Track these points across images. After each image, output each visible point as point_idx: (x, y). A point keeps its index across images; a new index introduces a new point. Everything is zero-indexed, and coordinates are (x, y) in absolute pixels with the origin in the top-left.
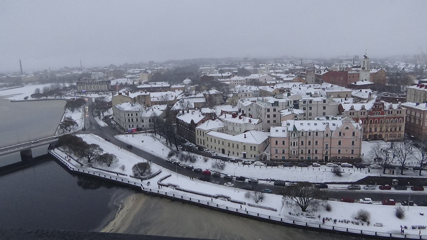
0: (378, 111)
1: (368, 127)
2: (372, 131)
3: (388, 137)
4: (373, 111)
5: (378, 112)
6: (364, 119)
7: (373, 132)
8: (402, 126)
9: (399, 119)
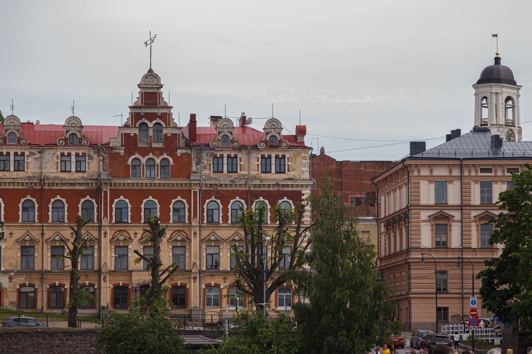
0: (159, 152)
2: (130, 269)
5: (158, 161)
6: (83, 194)
7: (131, 272)
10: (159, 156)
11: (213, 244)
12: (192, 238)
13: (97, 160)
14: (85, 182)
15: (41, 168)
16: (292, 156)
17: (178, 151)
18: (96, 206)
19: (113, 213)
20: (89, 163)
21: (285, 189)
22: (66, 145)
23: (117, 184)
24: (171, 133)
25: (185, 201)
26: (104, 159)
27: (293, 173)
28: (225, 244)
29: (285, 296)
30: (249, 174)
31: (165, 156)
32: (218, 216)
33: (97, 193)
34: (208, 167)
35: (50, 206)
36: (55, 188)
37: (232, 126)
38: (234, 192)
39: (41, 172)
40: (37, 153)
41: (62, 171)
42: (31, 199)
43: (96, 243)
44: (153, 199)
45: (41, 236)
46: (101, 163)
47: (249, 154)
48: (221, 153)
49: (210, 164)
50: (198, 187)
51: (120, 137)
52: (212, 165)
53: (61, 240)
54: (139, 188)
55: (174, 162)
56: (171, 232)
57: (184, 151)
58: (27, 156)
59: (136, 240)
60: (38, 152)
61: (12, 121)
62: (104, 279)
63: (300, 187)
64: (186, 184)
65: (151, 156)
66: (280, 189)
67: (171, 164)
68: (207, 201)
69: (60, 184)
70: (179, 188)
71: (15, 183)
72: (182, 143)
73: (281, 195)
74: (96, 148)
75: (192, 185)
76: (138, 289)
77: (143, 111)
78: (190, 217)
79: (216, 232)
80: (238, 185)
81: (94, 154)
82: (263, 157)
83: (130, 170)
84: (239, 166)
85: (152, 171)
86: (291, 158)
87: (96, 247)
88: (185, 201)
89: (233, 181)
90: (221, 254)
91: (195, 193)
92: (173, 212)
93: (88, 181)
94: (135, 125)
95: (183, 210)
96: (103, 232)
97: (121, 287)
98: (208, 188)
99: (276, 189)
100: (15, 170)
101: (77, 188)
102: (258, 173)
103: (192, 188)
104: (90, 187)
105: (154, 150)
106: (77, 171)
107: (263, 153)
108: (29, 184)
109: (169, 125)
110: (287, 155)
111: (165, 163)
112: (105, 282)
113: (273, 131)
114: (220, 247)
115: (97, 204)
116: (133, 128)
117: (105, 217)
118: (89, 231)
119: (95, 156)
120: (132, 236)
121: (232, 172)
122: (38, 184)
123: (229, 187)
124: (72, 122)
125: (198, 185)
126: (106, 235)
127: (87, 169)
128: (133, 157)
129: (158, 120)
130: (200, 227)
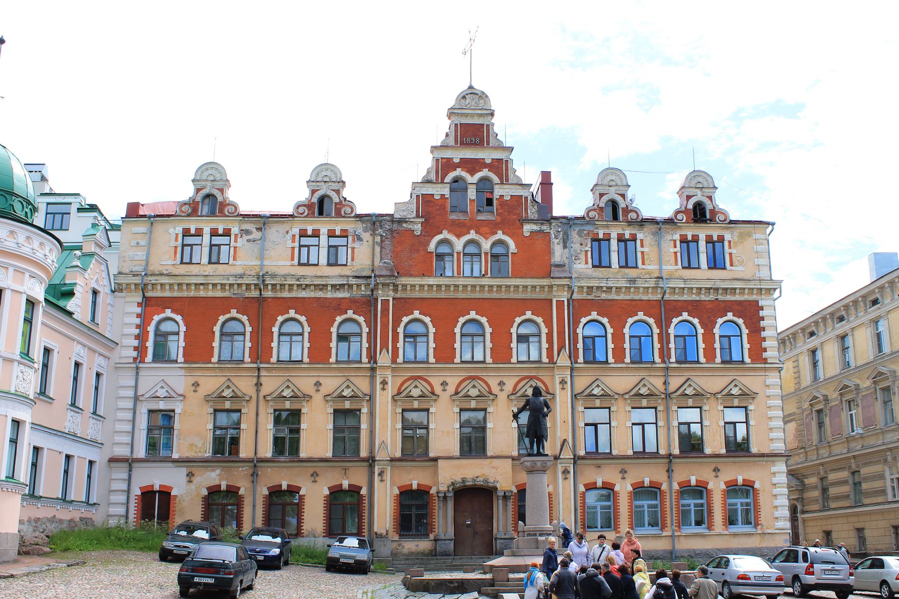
1: (384, 400)
2: (432, 454)
3: (624, 527)
4: (430, 229)
5: (486, 245)
6: (339, 306)
7: (435, 460)
8: (747, 395)
9: (709, 326)
10: (487, 235)
11: (598, 403)
12: (558, 391)
13: (371, 242)
14: (345, 283)
15: (262, 258)
16: (736, 238)
17: (525, 227)
18: (366, 330)
19: (400, 345)
20: (353, 249)
21: (729, 298)
22: (311, 214)
23: (409, 288)
24: (510, 194)
25: (539, 320)
26: (382, 241)
27: (740, 268)
28: (621, 402)
29: (739, 506)
30: (660, 270)
31: (500, 235)
32: (606, 350)
33: (367, 306)
34: (582, 256)
35: (275, 330)
36: (286, 294)
37: (625, 184)
38: (633, 303)
39: (262, 266)
40: (254, 230)
41: (300, 264)
42: (239, 316)
43: (365, 404)
44: (478, 317)
45: (254, 389)
46: (378, 249)
47: (657, 234)
48: (607, 231)
49: (586, 251)
50: (566, 293)
51: (415, 201)
52: (589, 254)
53: (295, 397)
54: (451, 295)
55: (517, 246)
56: (517, 379)
57: (535, 227)
58: (236, 235)
59: (445, 397)
60: (257, 229)
61: (210, 172)
62: (380, 474)
63: (757, 294)
64: (542, 287)
65: (472, 235)
66: (720, 297)
67: (511, 251)
68: (584, 320)
69: (295, 288)
70: (528, 295)
71: (208, 284)
72: (532, 212)
73: (722, 308)
74: (367, 221)
75: (555, 289)
76: (451, 494)
77: (457, 155)
78: (550, 350)
79: (602, 378)
80: (641, 290)
81: (365, 231)
82: (684, 240)
83: (432, 262)
84: (639, 255)
85: (476, 267)
86: (735, 243)
87: (365, 410)
88: (539, 320)
89: (633, 281)
90: (613, 424)
91: (560, 304)
92: (518, 342)
93: (353, 281)
94: (443, 179)
95: (536, 339)
96: (378, 380)
97: (414, 491)
98: (584, 296)
99: (712, 297)
100: (210, 263)
101: (329, 295)
102: (676, 267)
103: (554, 293)
104: (355, 293)
105: (478, 227)
106: (329, 264)
107: (683, 233)
108: (236, 286)
109: (507, 180)
110: (728, 237)
111: (499, 250)
112: (382, 481)
113: (699, 192)
114: (612, 409)
115: (369, 326)
116: (440, 185)
117: (384, 350)
118: (351, 379)
119: (366, 236)
120: (438, 389)
121: (626, 266)
122: (253, 287)
123: (625, 293)
124: (324, 173)
125: (566, 289)
126: (386, 387)
127: (349, 260)
128: (439, 237)
129: (485, 172)
130: (572, 369)
